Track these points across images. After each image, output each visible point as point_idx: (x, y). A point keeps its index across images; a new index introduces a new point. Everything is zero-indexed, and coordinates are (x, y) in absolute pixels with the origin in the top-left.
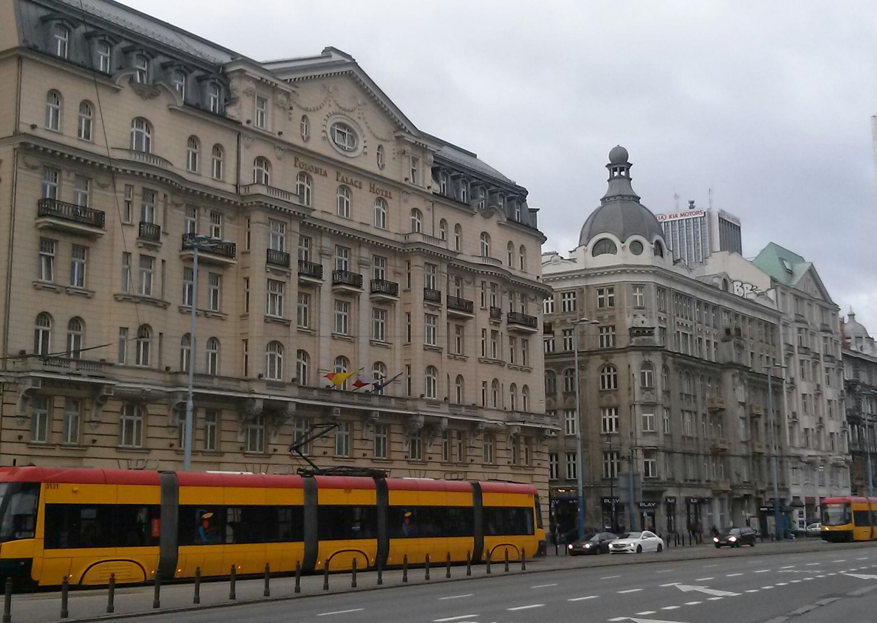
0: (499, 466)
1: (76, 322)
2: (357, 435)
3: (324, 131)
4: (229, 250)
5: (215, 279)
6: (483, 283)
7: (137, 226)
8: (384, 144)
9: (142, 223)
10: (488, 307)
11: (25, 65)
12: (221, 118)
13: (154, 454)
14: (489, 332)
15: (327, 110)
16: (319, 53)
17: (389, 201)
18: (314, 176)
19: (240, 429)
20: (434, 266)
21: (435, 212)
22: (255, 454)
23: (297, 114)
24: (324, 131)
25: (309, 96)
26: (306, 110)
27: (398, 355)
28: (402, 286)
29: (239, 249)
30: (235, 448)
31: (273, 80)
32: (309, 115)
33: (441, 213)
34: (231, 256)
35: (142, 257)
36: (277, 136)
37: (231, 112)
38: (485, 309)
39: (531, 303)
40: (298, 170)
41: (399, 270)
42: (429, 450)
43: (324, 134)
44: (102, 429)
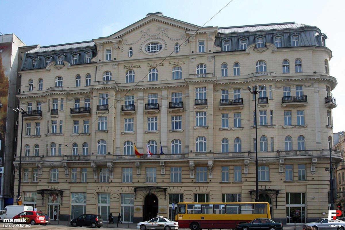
0: (308, 181)
1: (85, 144)
2: (308, 170)
3: (140, 49)
6: (271, 86)
8: (179, 42)
11: (216, 58)
13: (61, 184)
15: (143, 40)
17: (182, 66)
18: (134, 69)
19: (191, 174)
20: (205, 88)
21: (216, 61)
22: (55, 182)
23: (126, 48)
24: (140, 49)
25: (129, 39)
26: (131, 45)
30: (94, 181)
31: (108, 41)
32: (132, 46)
33: (220, 60)
36: (114, 61)
39: (305, 89)
40: (126, 70)
42: (210, 177)
43: (141, 51)
44: (43, 177)
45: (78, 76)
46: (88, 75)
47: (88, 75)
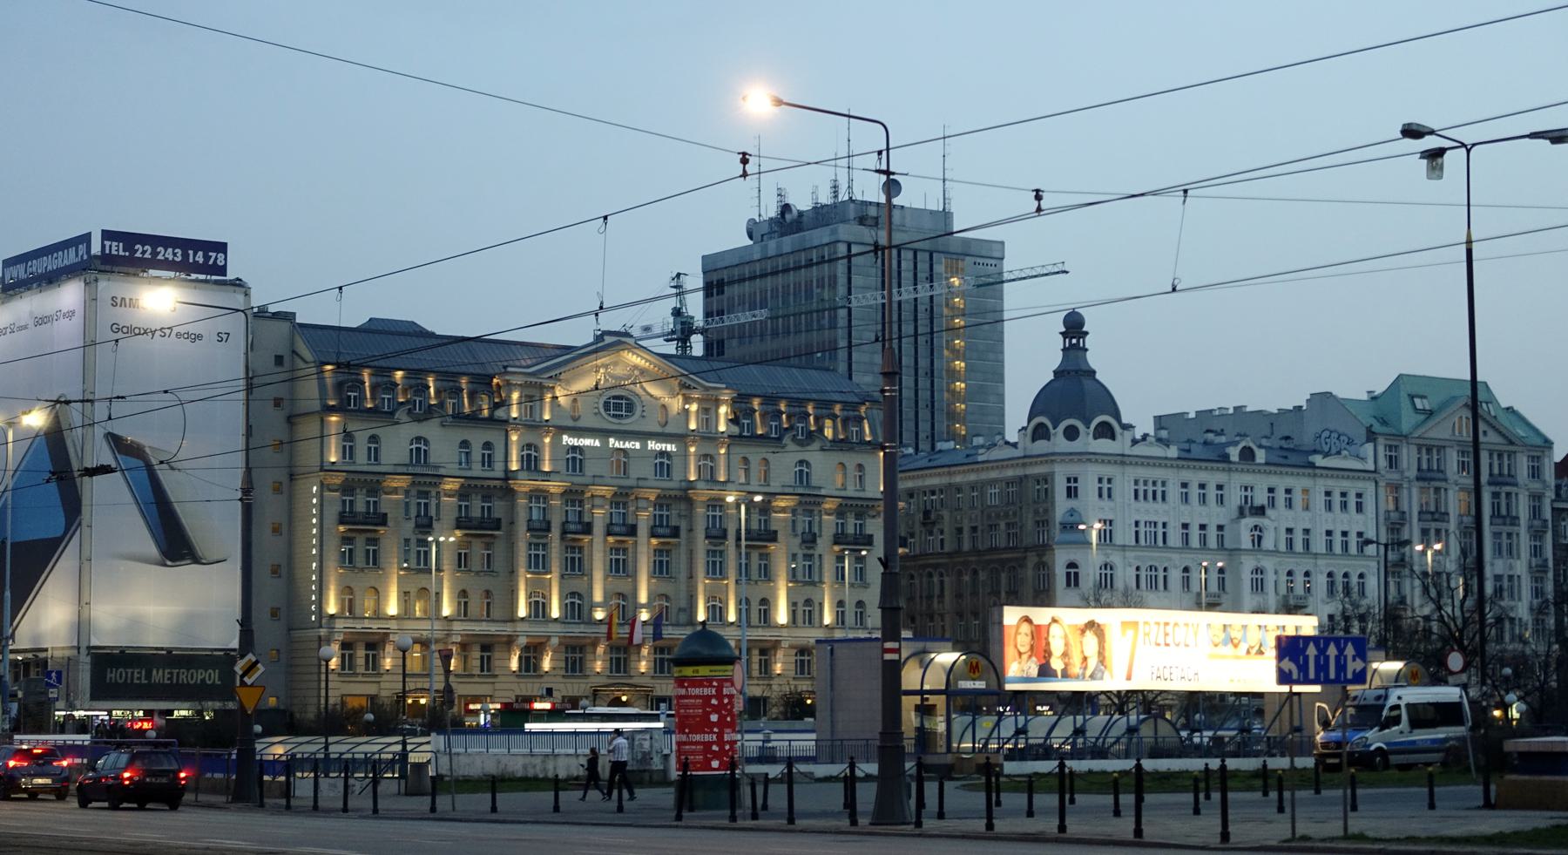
4: (497, 524)
5: (488, 546)
7: (414, 520)
9: (418, 516)
10: (800, 532)
12: (491, 420)
14: (800, 557)
16: (591, 340)
27: (683, 587)
28: (683, 526)
29: (504, 523)
34: (498, 528)
35: (418, 540)
37: (500, 413)
38: (796, 535)
41: (683, 513)
45: (465, 444)
46: (488, 445)
47: (488, 445)
